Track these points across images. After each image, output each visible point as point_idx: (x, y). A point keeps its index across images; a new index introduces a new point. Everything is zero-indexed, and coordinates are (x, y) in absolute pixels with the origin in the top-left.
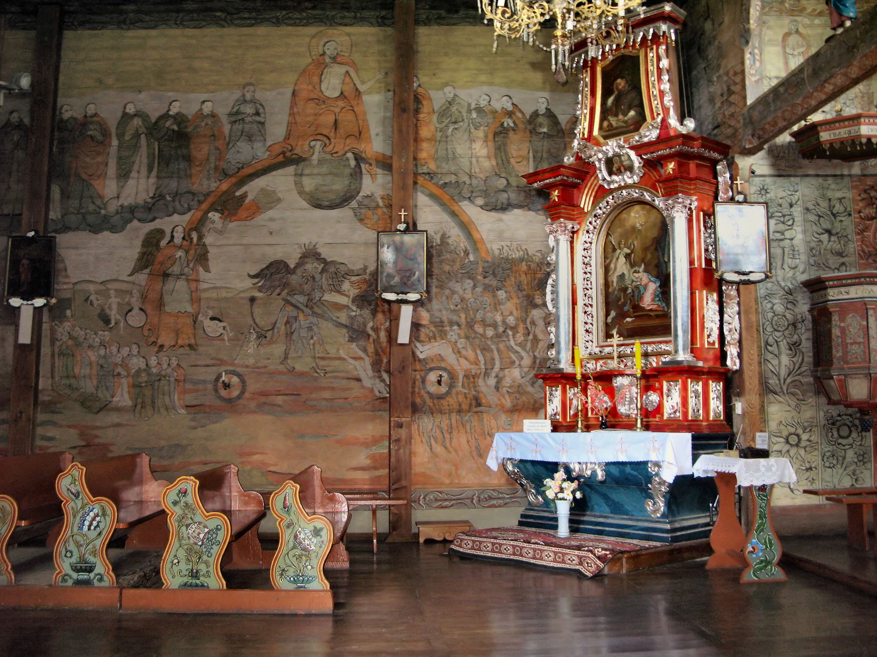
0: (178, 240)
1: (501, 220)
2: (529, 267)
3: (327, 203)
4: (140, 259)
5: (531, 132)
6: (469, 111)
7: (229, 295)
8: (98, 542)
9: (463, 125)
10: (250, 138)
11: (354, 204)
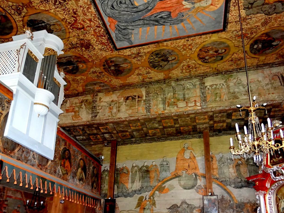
0: (147, 199)
1: (240, 191)
2: (251, 205)
3: (188, 188)
4: (137, 204)
5: (247, 164)
6: (227, 160)
9: (226, 164)
10: (166, 171)
11: (195, 188)
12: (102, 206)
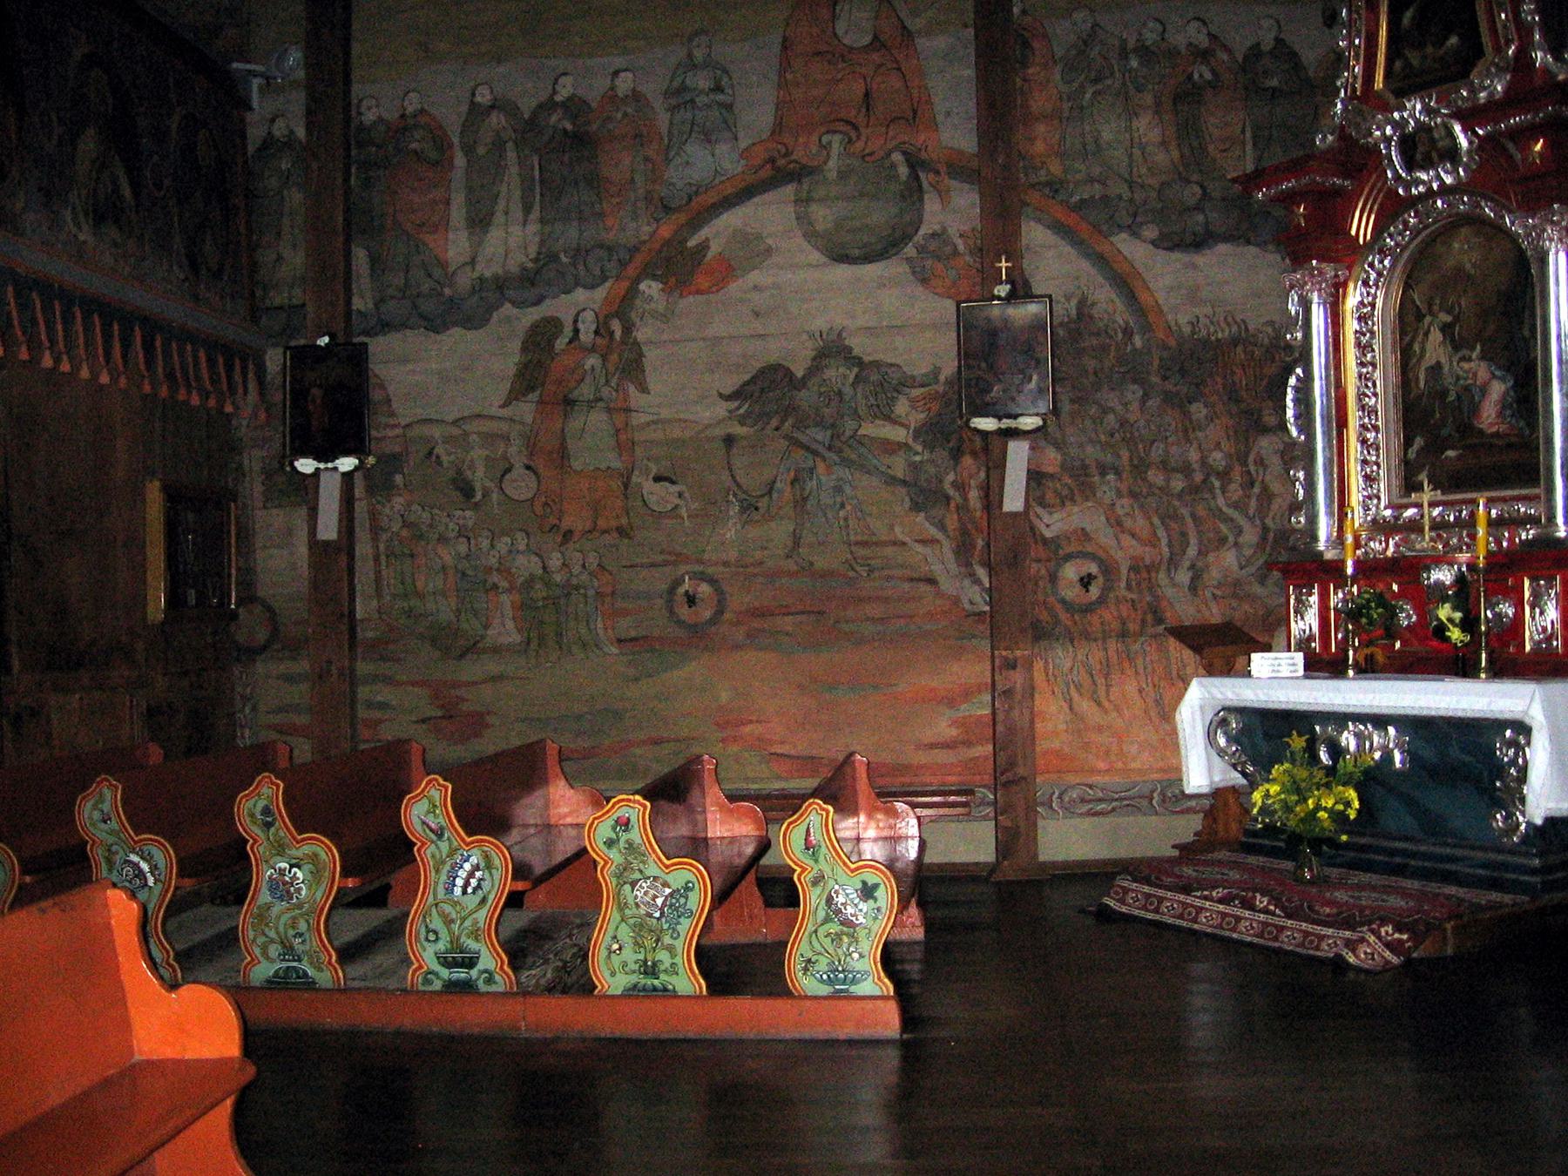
0: (586, 336)
3: (857, 252)
7: (688, 434)
8: (482, 915)
10: (708, 138)
11: (910, 250)
12: (278, 397)
